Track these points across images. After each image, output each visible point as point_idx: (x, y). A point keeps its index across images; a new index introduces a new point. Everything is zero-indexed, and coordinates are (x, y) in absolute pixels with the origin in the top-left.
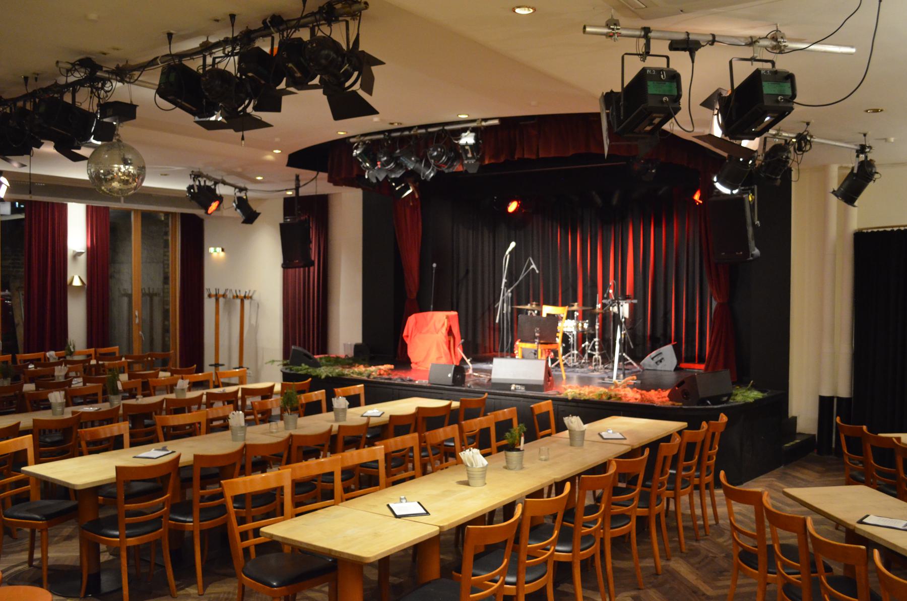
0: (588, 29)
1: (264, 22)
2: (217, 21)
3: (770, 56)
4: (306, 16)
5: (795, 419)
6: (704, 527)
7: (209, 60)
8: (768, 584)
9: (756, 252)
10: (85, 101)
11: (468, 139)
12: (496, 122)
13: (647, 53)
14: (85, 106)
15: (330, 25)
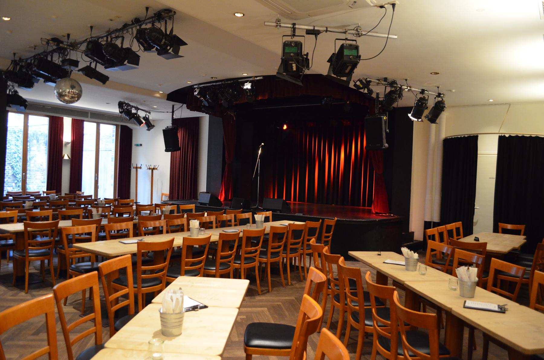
0: (266, 23)
1: (132, 21)
2: (111, 20)
3: (354, 38)
4: (148, 19)
5: (413, 233)
6: (303, 268)
7: (109, 39)
8: (329, 295)
9: (387, 145)
10: (57, 59)
11: (248, 86)
12: (261, 78)
13: (294, 35)
14: (56, 62)
15: (159, 22)
